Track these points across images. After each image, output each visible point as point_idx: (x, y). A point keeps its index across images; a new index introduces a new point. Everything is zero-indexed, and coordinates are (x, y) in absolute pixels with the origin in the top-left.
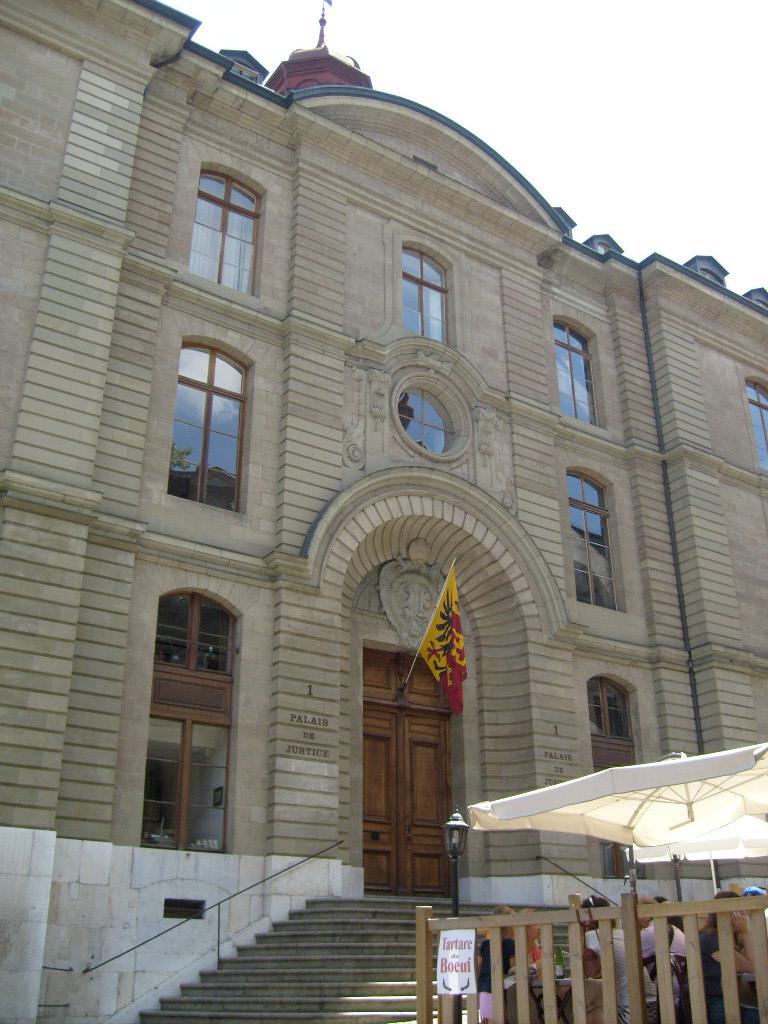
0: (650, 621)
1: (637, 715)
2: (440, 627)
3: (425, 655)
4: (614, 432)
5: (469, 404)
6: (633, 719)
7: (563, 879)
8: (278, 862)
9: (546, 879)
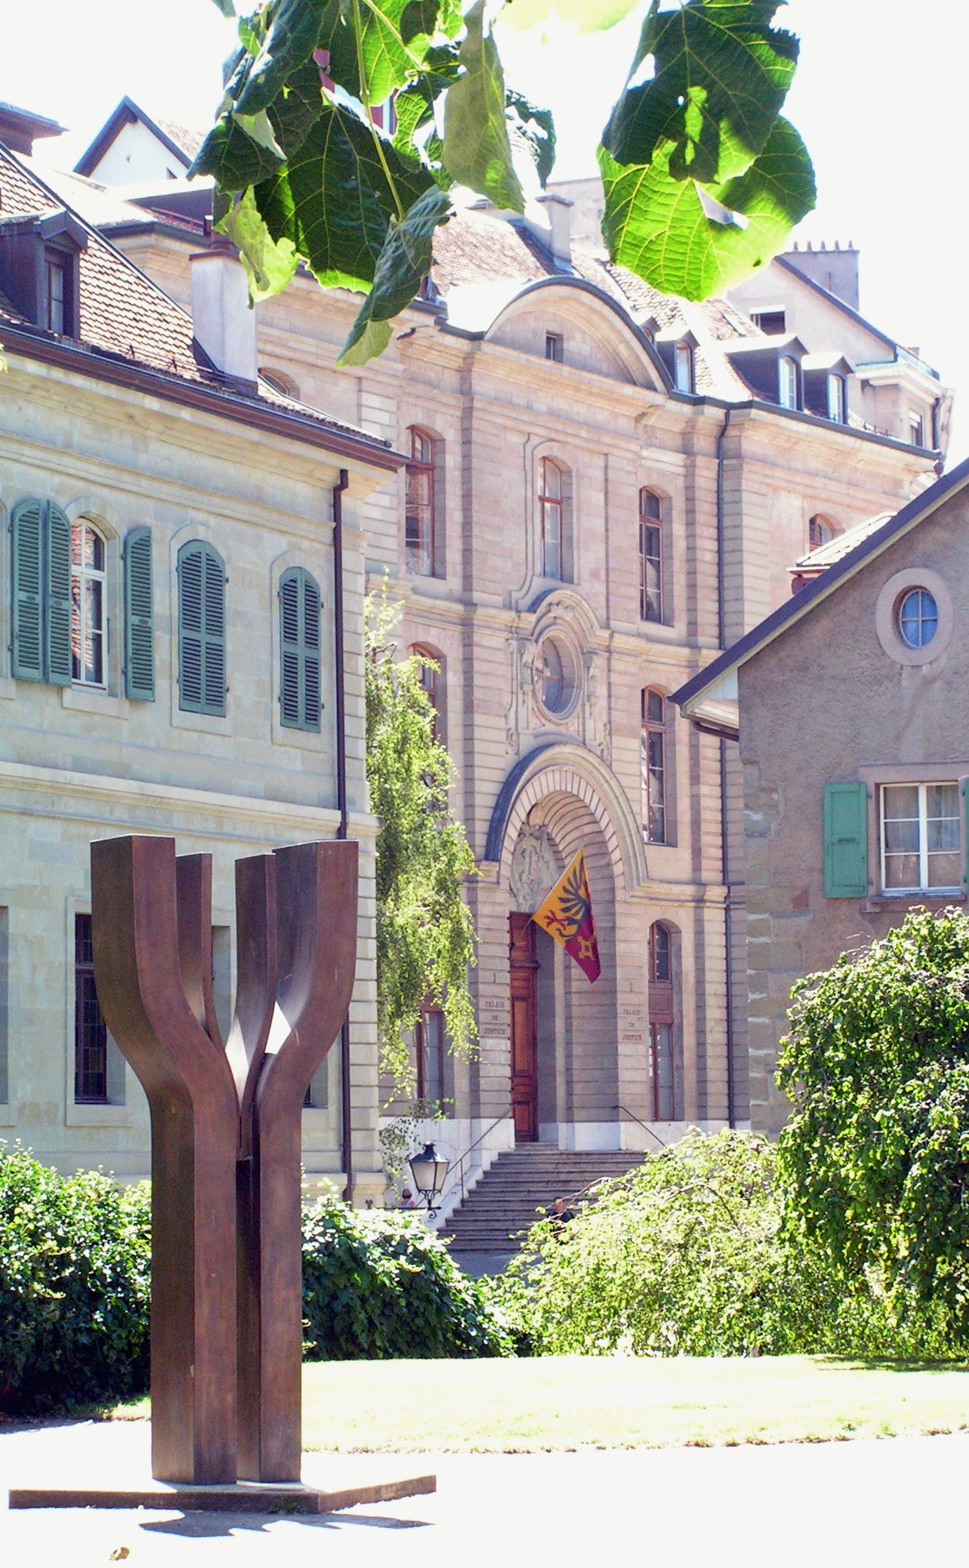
0: (697, 852)
1: (679, 958)
2: (562, 900)
3: (542, 923)
4: (679, 629)
5: (581, 648)
6: (674, 960)
7: (632, 1124)
8: (485, 1123)
9: (622, 1124)
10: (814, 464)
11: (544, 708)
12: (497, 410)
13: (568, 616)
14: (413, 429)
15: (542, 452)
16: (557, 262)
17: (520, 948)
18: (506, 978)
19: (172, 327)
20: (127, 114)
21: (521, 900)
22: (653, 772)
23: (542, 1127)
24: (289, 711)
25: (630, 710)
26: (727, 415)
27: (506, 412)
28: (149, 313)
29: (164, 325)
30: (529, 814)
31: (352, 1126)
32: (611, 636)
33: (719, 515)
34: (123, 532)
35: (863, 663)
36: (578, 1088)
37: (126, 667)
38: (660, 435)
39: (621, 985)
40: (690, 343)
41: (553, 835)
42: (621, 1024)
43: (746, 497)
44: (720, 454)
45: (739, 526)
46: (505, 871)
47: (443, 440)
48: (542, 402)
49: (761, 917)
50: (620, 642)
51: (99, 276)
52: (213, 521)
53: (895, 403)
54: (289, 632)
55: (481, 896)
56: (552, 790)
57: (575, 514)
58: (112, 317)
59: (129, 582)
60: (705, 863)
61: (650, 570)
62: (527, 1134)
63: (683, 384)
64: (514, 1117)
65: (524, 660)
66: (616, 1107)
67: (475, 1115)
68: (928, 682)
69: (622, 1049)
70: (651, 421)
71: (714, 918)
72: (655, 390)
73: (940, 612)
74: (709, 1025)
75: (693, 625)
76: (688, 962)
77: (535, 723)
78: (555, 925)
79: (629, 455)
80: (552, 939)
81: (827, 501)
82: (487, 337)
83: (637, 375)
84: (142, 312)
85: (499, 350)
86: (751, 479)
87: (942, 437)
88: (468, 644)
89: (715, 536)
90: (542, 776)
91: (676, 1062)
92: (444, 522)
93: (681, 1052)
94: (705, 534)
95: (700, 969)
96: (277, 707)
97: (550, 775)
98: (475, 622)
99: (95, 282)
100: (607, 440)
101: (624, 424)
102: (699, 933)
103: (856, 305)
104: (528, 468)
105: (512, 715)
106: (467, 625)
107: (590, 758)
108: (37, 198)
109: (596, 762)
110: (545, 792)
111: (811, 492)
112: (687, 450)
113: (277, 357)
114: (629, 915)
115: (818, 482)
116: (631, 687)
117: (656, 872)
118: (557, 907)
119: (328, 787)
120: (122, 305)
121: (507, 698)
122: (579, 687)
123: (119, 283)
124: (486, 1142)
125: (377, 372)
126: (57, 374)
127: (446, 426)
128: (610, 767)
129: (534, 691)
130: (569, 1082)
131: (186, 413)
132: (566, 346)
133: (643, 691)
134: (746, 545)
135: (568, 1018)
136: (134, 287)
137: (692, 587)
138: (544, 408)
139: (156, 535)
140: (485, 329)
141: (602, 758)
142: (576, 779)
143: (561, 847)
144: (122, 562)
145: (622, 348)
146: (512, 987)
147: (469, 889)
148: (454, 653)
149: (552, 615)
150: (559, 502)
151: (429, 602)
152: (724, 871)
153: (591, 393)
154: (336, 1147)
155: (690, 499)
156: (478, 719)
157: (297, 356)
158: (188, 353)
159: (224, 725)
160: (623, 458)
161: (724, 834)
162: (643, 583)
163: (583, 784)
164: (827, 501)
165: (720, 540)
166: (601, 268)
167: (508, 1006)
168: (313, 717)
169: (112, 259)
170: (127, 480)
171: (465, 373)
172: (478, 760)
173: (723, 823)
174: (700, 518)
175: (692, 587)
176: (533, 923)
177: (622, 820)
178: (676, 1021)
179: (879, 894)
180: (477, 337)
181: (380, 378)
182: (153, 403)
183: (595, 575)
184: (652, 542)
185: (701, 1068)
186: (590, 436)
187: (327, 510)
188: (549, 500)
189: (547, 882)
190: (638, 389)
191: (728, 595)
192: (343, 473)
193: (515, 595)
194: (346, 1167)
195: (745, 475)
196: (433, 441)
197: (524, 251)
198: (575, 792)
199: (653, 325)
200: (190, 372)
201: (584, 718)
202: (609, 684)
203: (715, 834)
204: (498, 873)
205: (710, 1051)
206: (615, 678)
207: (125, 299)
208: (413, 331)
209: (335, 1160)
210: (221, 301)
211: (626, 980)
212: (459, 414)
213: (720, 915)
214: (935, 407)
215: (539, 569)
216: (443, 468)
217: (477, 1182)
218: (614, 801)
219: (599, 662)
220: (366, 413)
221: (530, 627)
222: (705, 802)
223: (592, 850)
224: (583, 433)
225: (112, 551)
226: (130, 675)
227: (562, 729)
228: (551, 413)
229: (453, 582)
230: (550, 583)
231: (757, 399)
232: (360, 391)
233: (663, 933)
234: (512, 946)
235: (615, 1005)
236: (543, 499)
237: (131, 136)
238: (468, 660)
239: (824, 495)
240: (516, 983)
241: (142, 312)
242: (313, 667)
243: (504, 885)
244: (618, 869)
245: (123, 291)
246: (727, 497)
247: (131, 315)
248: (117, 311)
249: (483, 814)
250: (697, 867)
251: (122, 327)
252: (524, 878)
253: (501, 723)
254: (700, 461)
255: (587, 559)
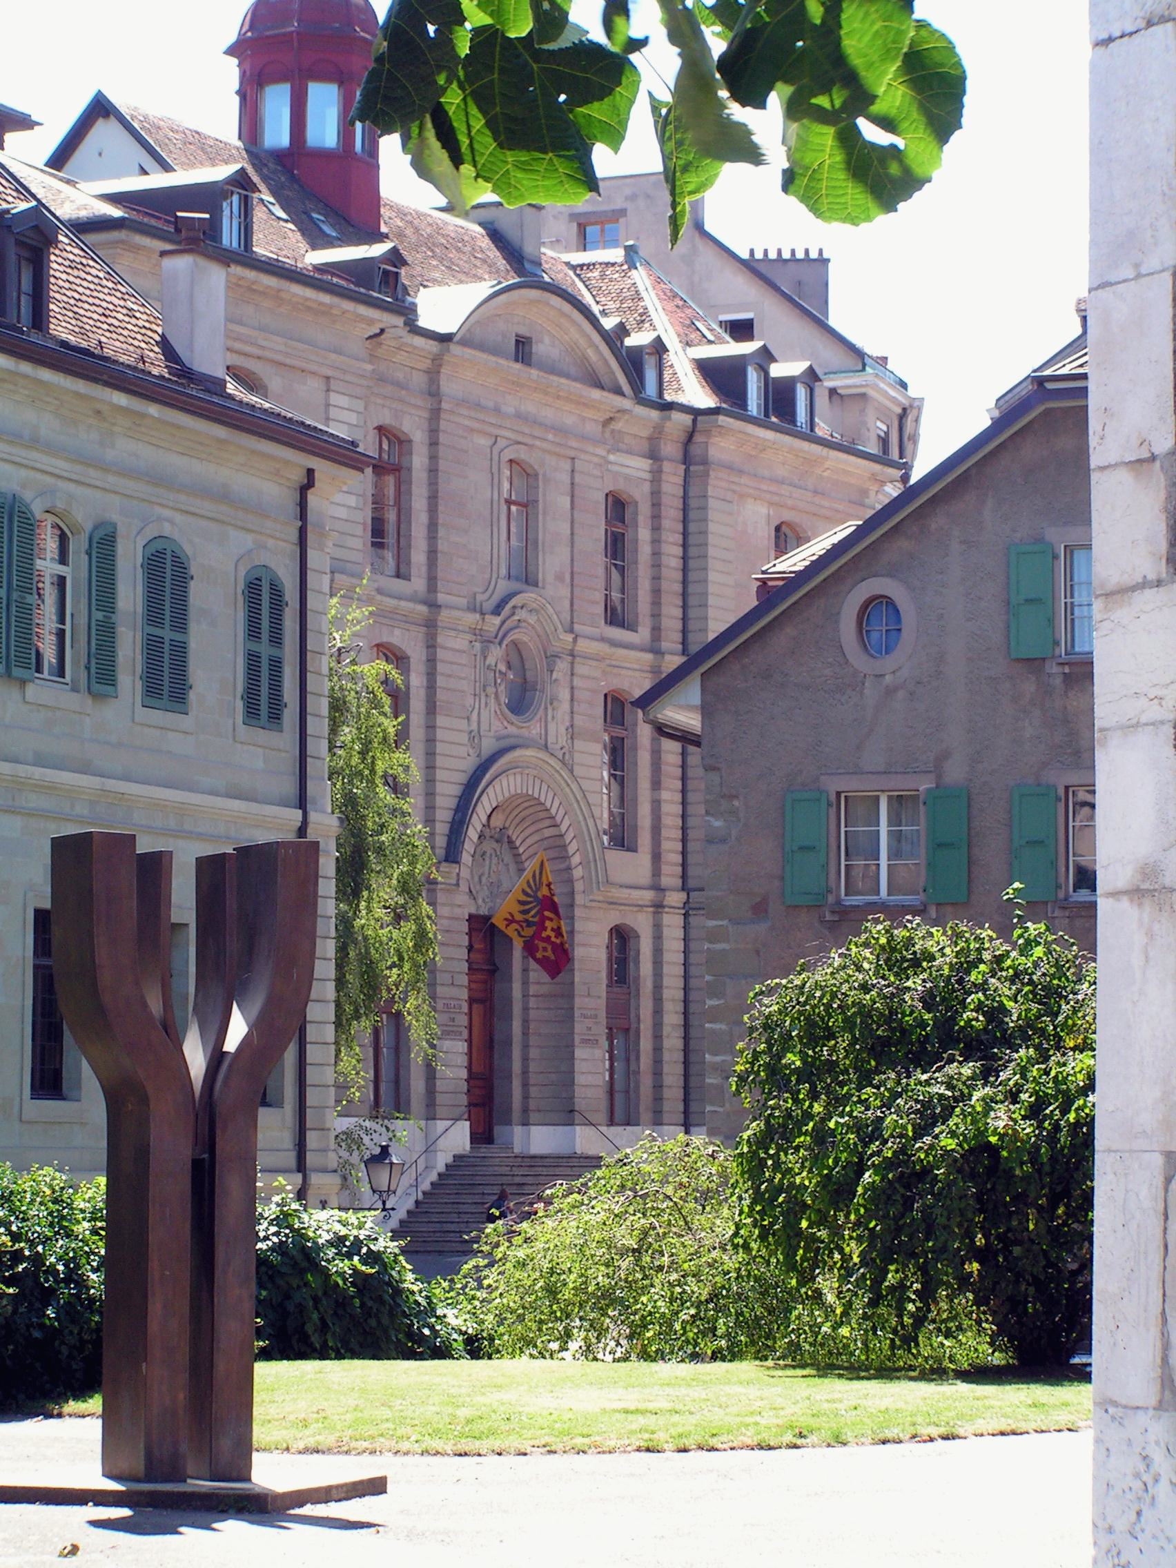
0: (656, 857)
1: (637, 963)
2: (521, 903)
3: (501, 925)
4: (643, 634)
8: (441, 1125)
9: (578, 1128)
10: (781, 472)
11: (507, 711)
12: (465, 412)
13: (532, 620)
14: (380, 429)
15: (509, 454)
16: (527, 265)
17: (479, 951)
18: (464, 980)
19: (141, 323)
20: (100, 109)
21: (480, 901)
22: (614, 776)
23: (497, 1130)
24: (252, 711)
25: (592, 715)
26: (694, 421)
27: (473, 414)
28: (119, 309)
29: (133, 321)
30: (489, 816)
31: (308, 1125)
32: (575, 640)
33: (685, 521)
34: (88, 527)
35: (827, 672)
36: (534, 1091)
37: (89, 662)
38: (627, 439)
39: (579, 989)
40: (659, 347)
41: (514, 838)
42: (579, 1028)
43: (712, 503)
44: (687, 459)
45: (704, 533)
46: (465, 873)
47: (410, 441)
48: (510, 405)
49: (721, 923)
50: (582, 645)
51: (69, 270)
52: (179, 518)
53: (862, 411)
54: (253, 631)
55: (441, 897)
56: (513, 792)
57: (540, 517)
58: (81, 312)
59: (94, 578)
60: (665, 869)
61: (615, 575)
62: (482, 1136)
63: (651, 389)
64: (469, 1119)
65: (487, 663)
66: (572, 1111)
67: (431, 1117)
68: (890, 691)
69: (579, 1053)
70: (618, 426)
71: (673, 924)
72: (623, 394)
73: (903, 620)
74: (666, 1030)
75: (656, 631)
76: (646, 968)
77: (497, 726)
78: (515, 926)
79: (596, 460)
80: (511, 940)
81: (793, 508)
82: (456, 339)
83: (605, 380)
84: (111, 307)
85: (469, 352)
86: (717, 485)
87: (908, 446)
88: (431, 646)
89: (681, 542)
90: (503, 778)
91: (633, 1066)
92: (409, 523)
93: (638, 1058)
94: (671, 539)
95: (658, 975)
96: (240, 705)
97: (511, 778)
98: (439, 624)
99: (64, 276)
100: (574, 444)
101: (592, 429)
102: (658, 937)
103: (826, 314)
104: (495, 470)
105: (474, 716)
106: (431, 627)
107: (552, 761)
108: (9, 191)
109: (558, 765)
110: (507, 795)
111: (776, 499)
112: (654, 455)
113: (246, 355)
114: (588, 919)
115: (785, 490)
116: (594, 691)
117: (617, 875)
118: (516, 909)
119: (289, 786)
120: (91, 300)
121: (469, 700)
122: (542, 691)
123: (89, 278)
124: (441, 1143)
125: (345, 372)
126: (26, 367)
127: (413, 427)
128: (571, 771)
129: (496, 694)
130: (525, 1085)
131: (154, 410)
132: (534, 350)
133: (606, 695)
134: (711, 552)
135: (526, 1022)
136: (104, 282)
137: (656, 592)
138: (511, 410)
139: (121, 530)
140: (454, 331)
141: (563, 762)
142: (538, 782)
143: (521, 850)
144: (87, 557)
145: (590, 352)
146: (470, 990)
147: (428, 890)
148: (417, 655)
149: (516, 618)
150: (525, 506)
151: (393, 602)
152: (684, 876)
153: (558, 397)
154: (291, 1146)
155: (656, 505)
156: (441, 720)
157: (268, 354)
158: (156, 349)
159: (186, 722)
160: (590, 462)
161: (684, 840)
162: (608, 587)
163: (544, 787)
164: (793, 508)
165: (685, 546)
166: (571, 273)
167: (465, 1008)
168: (275, 716)
169: (82, 254)
170: (93, 475)
171: (433, 373)
172: (440, 761)
173: (684, 829)
174: (666, 523)
175: (656, 592)
176: (493, 925)
177: (583, 823)
178: (634, 1026)
179: (839, 902)
180: (446, 339)
181: (348, 378)
182: (120, 399)
183: (559, 578)
184: (617, 547)
185: (658, 1073)
186: (557, 440)
187: (293, 509)
188: (515, 503)
189: (506, 885)
190: (605, 394)
191: (692, 601)
192: (310, 472)
193: (480, 598)
194: (301, 1167)
195: (711, 481)
196: (401, 442)
197: (494, 254)
198: (536, 795)
199: (622, 330)
200: (158, 368)
201: (546, 722)
202: (572, 688)
203: (675, 839)
204: (458, 875)
205: (666, 1056)
206: (577, 682)
207: (95, 294)
208: (382, 331)
209: (290, 1159)
210: (191, 297)
211: (585, 984)
212: (426, 415)
213: (679, 920)
214: (902, 417)
215: (503, 571)
216: (409, 470)
217: (432, 1184)
218: (575, 805)
219: (562, 666)
220: (333, 412)
221: (493, 630)
222: (666, 808)
223: (552, 854)
224: (550, 437)
225: (77, 546)
226: (93, 670)
227: (524, 732)
228: (519, 416)
229: (418, 583)
230: (515, 586)
231: (724, 406)
232: (328, 390)
233: (622, 938)
234: (470, 948)
235: (572, 1009)
236: (509, 502)
237: (103, 131)
238: (432, 661)
239: (790, 502)
240: (473, 986)
241: (111, 307)
242: (276, 666)
243: (464, 887)
244: (578, 873)
245: (92, 286)
246: (693, 503)
247: (100, 310)
248: (86, 306)
249: (444, 815)
250: (656, 872)
251: (91, 322)
252: (484, 880)
253: (463, 724)
254: (667, 467)
255: (552, 563)
